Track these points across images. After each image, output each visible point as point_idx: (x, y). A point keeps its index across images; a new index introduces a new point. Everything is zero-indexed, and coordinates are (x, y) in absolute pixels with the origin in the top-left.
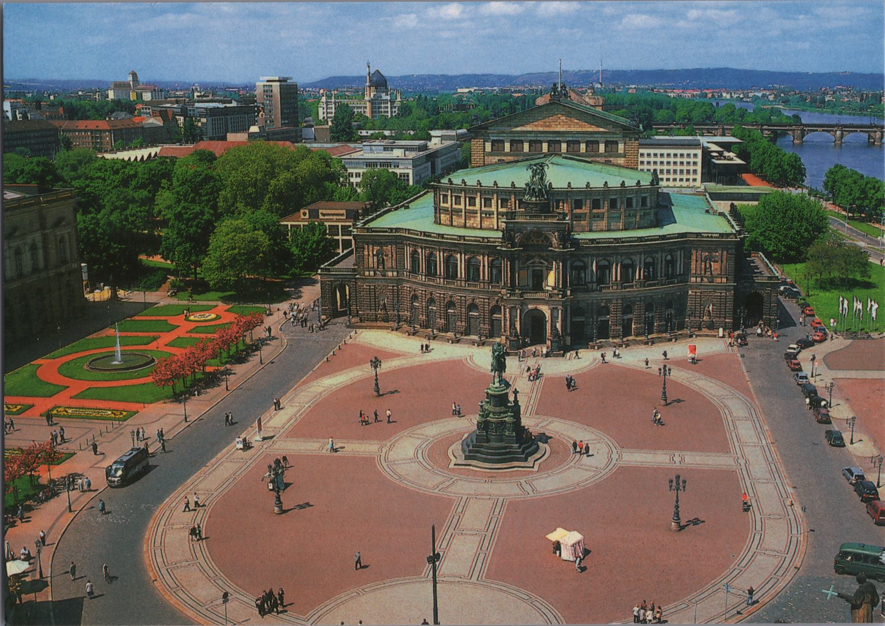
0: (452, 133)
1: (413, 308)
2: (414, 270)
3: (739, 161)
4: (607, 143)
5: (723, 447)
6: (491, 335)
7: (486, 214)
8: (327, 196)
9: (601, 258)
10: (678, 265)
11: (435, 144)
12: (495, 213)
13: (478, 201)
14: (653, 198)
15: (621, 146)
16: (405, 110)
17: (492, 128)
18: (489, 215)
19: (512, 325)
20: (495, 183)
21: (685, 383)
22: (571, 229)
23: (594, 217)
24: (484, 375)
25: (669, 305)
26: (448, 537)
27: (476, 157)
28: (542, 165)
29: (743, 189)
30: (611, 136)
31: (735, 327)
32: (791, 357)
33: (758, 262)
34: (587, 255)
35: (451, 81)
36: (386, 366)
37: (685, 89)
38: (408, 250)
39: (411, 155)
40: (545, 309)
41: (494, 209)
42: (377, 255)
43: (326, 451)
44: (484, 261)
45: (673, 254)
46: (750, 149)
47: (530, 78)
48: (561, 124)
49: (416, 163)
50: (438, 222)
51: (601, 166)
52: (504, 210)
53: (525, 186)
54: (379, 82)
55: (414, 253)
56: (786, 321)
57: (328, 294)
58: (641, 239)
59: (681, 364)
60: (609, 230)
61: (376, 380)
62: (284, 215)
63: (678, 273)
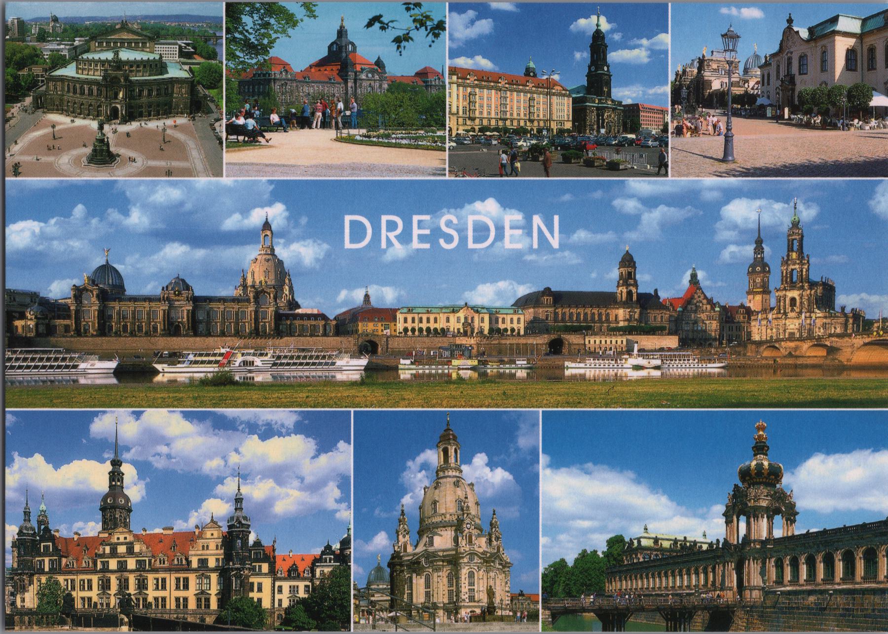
0: (83, 39)
1: (68, 106)
2: (69, 91)
3: (192, 50)
4: (142, 43)
5: (186, 158)
6: (98, 116)
8: (36, 63)
11: (76, 43)
16: (65, 31)
19: (106, 112)
22: (128, 76)
24: (95, 132)
25: (166, 105)
27: (92, 47)
29: (194, 61)
31: (191, 113)
32: (212, 125)
33: (199, 89)
35: (83, 19)
37: (172, 22)
38: (66, 83)
39: (67, 47)
40: (119, 106)
43: (35, 160)
44: (95, 88)
46: (197, 45)
47: (112, 18)
48: (125, 36)
49: (69, 50)
50: (77, 73)
54: (55, 19)
55: (68, 85)
56: (209, 111)
57: (36, 99)
58: (155, 80)
59: (170, 127)
60: (143, 76)
62: (20, 69)
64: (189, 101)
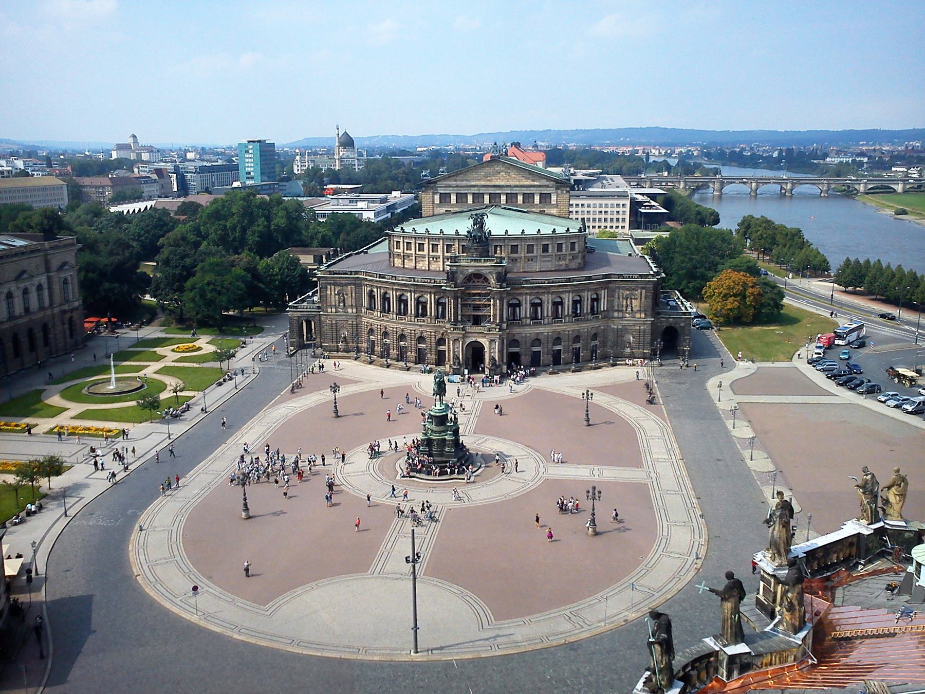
2: (371, 308)
7: (433, 259)
9: (533, 297)
10: (602, 303)
12: (441, 257)
13: (426, 246)
14: (581, 242)
15: (554, 198)
17: (440, 183)
18: (436, 259)
20: (441, 231)
21: (605, 406)
23: (529, 260)
26: (393, 539)
27: (426, 210)
28: (482, 215)
30: (545, 189)
34: (521, 294)
36: (343, 391)
38: (366, 290)
40: (484, 342)
41: (440, 253)
42: (339, 294)
45: (598, 292)
51: (536, 216)
52: (449, 254)
53: (466, 234)
61: (335, 403)
63: (602, 309)
64: (647, 328)
